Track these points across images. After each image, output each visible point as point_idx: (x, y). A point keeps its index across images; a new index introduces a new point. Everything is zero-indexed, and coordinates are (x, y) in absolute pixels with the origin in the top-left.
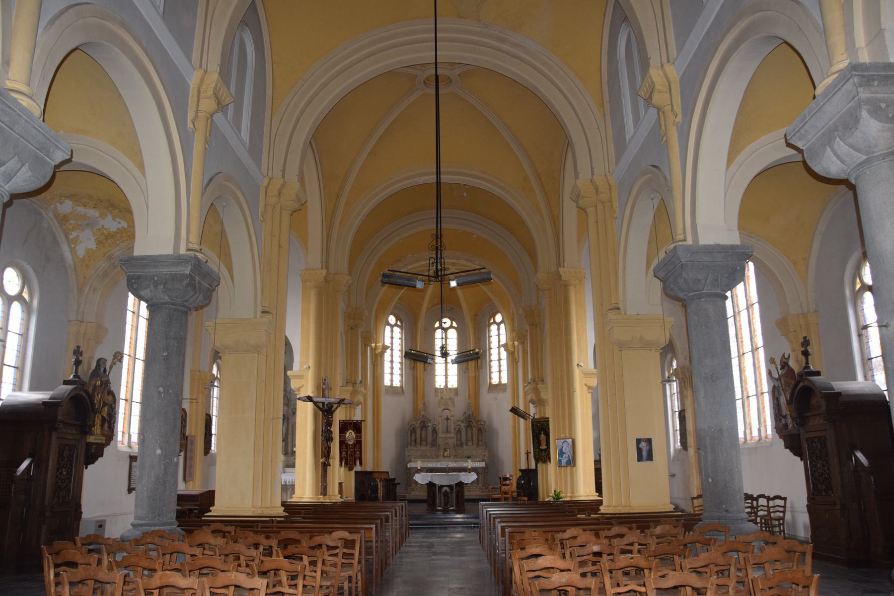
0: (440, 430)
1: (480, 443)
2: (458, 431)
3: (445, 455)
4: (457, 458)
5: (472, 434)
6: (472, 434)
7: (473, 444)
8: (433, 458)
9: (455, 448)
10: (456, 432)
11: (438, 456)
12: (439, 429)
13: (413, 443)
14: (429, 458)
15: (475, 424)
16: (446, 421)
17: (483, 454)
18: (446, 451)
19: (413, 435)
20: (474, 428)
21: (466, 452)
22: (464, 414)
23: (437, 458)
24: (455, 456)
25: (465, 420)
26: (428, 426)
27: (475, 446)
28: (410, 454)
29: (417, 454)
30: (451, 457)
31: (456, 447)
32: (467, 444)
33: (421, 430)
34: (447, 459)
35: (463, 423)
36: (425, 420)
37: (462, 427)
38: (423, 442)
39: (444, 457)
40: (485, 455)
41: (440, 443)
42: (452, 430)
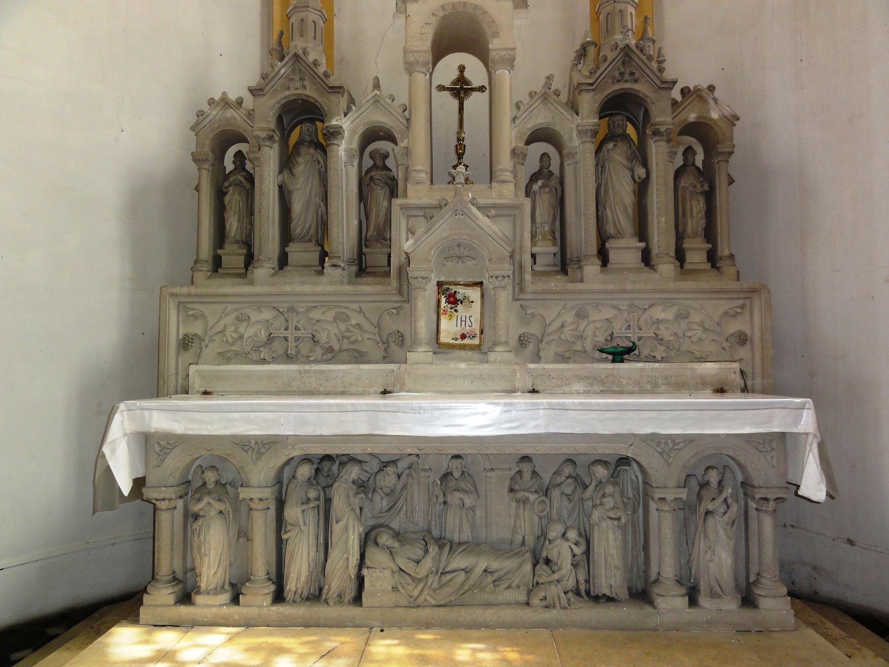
0: (420, 163)
1: (696, 257)
2: (534, 178)
3: (449, 328)
4: (537, 358)
5: (642, 188)
6: (642, 188)
7: (647, 258)
8: (359, 357)
9: (520, 286)
10: (524, 181)
11: (401, 339)
12: (407, 152)
13: (233, 257)
14: (331, 355)
15: (662, 117)
16: (455, 103)
17: (734, 327)
18: (453, 300)
19: (233, 199)
20: (657, 150)
21: (607, 313)
22: (582, 53)
23: (386, 359)
24: (522, 342)
25: (592, 87)
26: (336, 133)
27: (667, 268)
28: (197, 328)
29: (249, 332)
30: (499, 354)
31: (528, 277)
32: (603, 256)
33: (287, 163)
34: (461, 366)
35: (573, 107)
36: (310, 92)
37: (574, 142)
38: (292, 248)
39: (440, 348)
40: (742, 339)
41: (408, 245)
42: (505, 161)
